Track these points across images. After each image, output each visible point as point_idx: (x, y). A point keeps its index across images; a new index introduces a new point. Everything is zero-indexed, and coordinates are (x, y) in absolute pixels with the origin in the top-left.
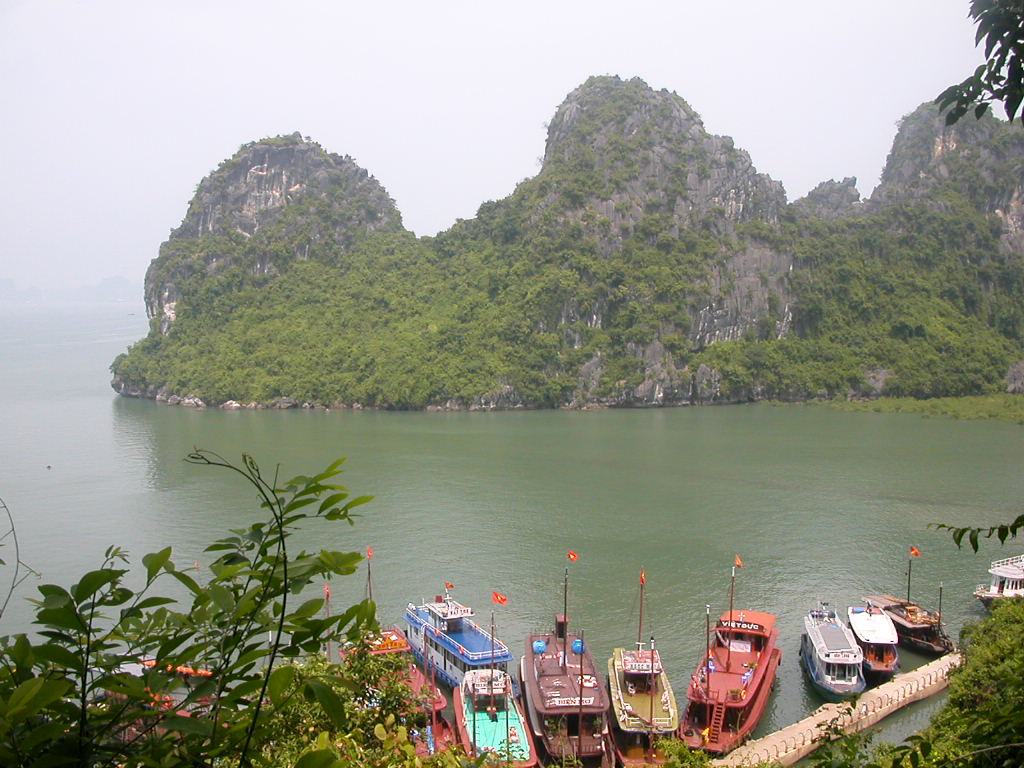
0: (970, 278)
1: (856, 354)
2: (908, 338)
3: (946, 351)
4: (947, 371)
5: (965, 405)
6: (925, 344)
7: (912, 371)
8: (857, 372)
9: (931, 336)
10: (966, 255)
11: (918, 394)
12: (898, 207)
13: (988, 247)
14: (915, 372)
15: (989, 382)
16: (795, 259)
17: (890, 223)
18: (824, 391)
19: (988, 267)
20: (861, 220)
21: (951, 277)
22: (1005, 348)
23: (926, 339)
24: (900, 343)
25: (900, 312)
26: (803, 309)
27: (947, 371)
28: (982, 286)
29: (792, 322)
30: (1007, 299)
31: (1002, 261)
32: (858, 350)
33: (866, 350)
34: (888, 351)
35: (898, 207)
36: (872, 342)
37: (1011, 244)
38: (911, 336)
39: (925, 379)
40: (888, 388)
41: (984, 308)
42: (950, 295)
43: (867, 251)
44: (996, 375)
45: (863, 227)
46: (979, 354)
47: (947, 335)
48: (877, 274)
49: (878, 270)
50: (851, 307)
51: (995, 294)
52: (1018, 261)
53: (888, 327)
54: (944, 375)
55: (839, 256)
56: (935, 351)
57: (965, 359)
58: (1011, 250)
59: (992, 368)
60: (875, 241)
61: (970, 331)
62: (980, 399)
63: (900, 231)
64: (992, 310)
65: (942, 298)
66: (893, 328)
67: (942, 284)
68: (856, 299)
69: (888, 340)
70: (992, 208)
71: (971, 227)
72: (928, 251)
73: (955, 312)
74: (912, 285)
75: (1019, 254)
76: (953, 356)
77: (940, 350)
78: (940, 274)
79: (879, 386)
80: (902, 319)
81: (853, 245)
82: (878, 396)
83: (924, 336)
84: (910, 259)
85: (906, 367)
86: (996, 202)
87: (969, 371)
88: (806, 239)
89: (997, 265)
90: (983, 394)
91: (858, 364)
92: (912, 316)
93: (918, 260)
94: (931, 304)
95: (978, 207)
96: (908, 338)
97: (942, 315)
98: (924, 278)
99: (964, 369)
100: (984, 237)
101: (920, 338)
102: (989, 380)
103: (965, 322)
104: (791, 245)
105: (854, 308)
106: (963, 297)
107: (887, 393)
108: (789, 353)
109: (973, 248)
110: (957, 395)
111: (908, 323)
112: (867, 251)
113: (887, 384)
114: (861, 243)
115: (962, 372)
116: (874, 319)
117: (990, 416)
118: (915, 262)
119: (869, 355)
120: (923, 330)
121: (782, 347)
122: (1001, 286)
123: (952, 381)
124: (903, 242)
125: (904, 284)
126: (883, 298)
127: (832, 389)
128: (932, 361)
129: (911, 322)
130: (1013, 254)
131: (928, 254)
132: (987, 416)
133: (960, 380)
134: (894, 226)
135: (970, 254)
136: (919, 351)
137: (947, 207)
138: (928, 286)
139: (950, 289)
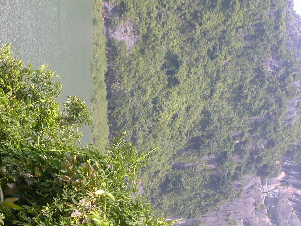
0: (221, 143)
1: (149, 14)
3: (154, 108)
4: (134, 108)
6: (161, 87)
7: (133, 71)
8: (131, 13)
9: (168, 94)
10: (244, 139)
12: (294, 68)
13: (251, 160)
14: (132, 74)
17: (277, 59)
19: (231, 161)
21: (223, 122)
22: (157, 172)
23: (164, 88)
25: (190, 65)
27: (134, 108)
28: (213, 156)
30: (199, 184)
31: (235, 177)
33: (153, 25)
34: (153, 47)
35: (294, 68)
36: (162, 32)
37: (252, 187)
38: (169, 73)
40: (116, 44)
41: (191, 158)
42: (206, 121)
43: (252, 32)
45: (277, 28)
48: (229, 42)
49: (233, 44)
50: (196, 12)
51: (204, 170)
53: (176, 51)
54: (130, 105)
56: (153, 97)
57: (145, 127)
58: (246, 188)
60: (262, 40)
63: (269, 69)
64: (188, 167)
65: (203, 112)
66: (176, 56)
67: (215, 112)
68: (205, 17)
69: (164, 49)
70: (286, 169)
71: (271, 144)
72: (249, 98)
73: (190, 122)
74: (218, 78)
75: (242, 195)
76: (149, 116)
77: (154, 102)
78: (226, 111)
79: (117, 36)
80: (185, 64)
81: (258, 16)
82: (107, 35)
83: (169, 86)
84: (242, 80)
85: (138, 64)
86: (292, 172)
87: (135, 131)
89: (232, 172)
92: (188, 76)
93: (240, 88)
94: (199, 99)
95: (289, 154)
96: (165, 71)
97: (188, 109)
98: (223, 93)
99: (137, 126)
100: (261, 157)
101: (166, 82)
103: (180, 133)
105: (195, 16)
106: (202, 136)
107: (110, 43)
109: (250, 147)
110: (110, 116)
111: (181, 70)
112: (252, 32)
114: (261, 25)
115: (134, 124)
116: (184, 37)
118: (239, 84)
119: (148, 28)
122: (211, 176)
123: (124, 114)
124: (259, 73)
125: (218, 71)
126: (204, 48)
128: (145, 92)
129: (182, 73)
131: (246, 97)
133: (125, 122)
134: (275, 63)
135: (245, 143)
136: (155, 79)
137: (290, 120)
138: (216, 97)
139: (212, 121)
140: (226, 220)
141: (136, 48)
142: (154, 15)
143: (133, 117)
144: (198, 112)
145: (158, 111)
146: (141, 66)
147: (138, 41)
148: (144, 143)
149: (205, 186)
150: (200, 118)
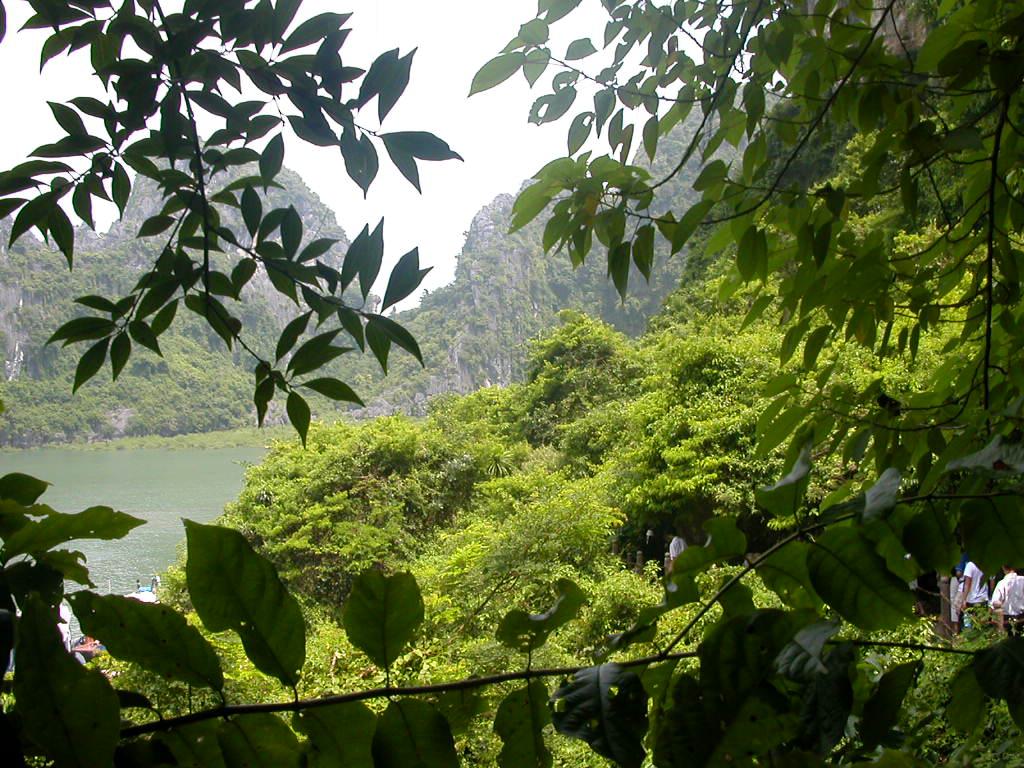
1: (96, 394)
2: (151, 375)
3: (191, 386)
4: (192, 407)
5: (212, 438)
8: (97, 412)
9: (175, 372)
11: (165, 432)
14: (158, 409)
15: (236, 416)
16: (25, 292)
17: (129, 259)
18: (62, 434)
20: (100, 254)
23: (170, 376)
24: (142, 381)
26: (36, 348)
27: (192, 407)
29: (23, 363)
30: (252, 338)
32: (97, 390)
33: (107, 390)
34: (131, 389)
38: (153, 372)
39: (170, 415)
44: (242, 408)
45: (100, 261)
46: (224, 389)
47: (191, 372)
52: (261, 299)
54: (190, 411)
55: (73, 290)
59: (238, 401)
60: (112, 276)
61: (215, 367)
62: (228, 434)
63: (139, 267)
65: (185, 336)
67: (184, 322)
73: (199, 349)
75: (261, 293)
76: (198, 392)
77: (185, 387)
79: (122, 426)
82: (121, 436)
83: (167, 372)
85: (149, 404)
88: (38, 271)
90: (230, 428)
91: (97, 404)
96: (151, 375)
97: (185, 352)
99: (210, 403)
102: (236, 414)
103: (210, 359)
104: (20, 278)
107: (129, 433)
108: (20, 396)
111: (150, 360)
113: (130, 423)
117: (238, 445)
120: (166, 367)
121: (13, 389)
127: (71, 432)
128: (176, 396)
130: (258, 294)
132: (234, 445)
133: (207, 415)
136: (162, 387)
140: (286, 308)
141: (131, 407)
142: (97, 390)
143: (202, 407)
144: (185, 340)
145: (194, 382)
146: (151, 401)
147: (124, 404)
148: (225, 396)
149: (254, 331)
150: (191, 339)
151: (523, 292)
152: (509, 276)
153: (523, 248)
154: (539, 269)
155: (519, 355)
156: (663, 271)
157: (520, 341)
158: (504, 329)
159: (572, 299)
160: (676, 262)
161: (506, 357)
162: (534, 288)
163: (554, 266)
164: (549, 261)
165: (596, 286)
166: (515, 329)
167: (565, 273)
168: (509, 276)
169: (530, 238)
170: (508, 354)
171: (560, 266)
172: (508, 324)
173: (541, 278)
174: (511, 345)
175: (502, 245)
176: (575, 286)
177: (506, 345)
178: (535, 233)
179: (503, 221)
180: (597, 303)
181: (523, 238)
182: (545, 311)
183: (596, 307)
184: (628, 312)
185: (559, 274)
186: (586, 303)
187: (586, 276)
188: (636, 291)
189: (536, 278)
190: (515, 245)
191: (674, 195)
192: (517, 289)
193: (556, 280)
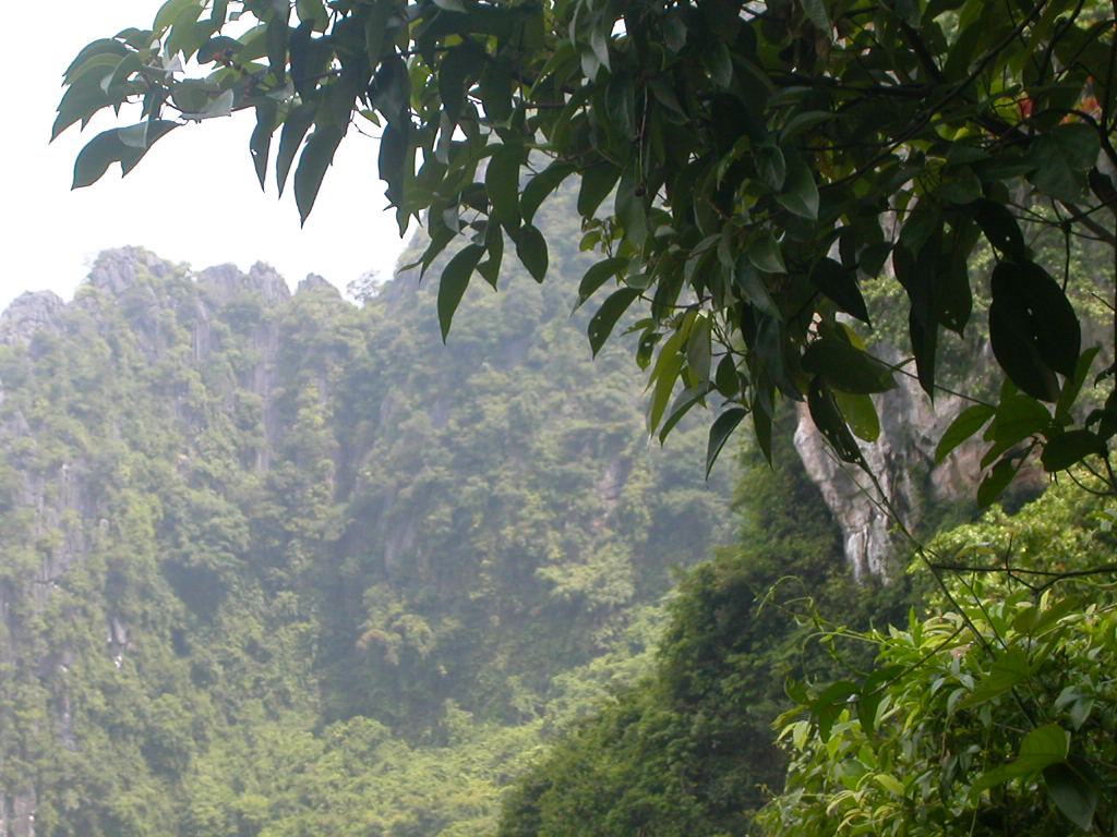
151: (86, 595)
152: (44, 549)
153: (88, 459)
154: (134, 521)
155: (61, 786)
156: (501, 539)
157: (69, 741)
158: (20, 705)
159: (230, 612)
160: (541, 516)
161: (23, 792)
162: (116, 579)
163: (182, 513)
164: (166, 499)
165: (304, 574)
166: (55, 704)
167: (213, 536)
168: (44, 549)
169: (112, 430)
170: (28, 783)
171: (199, 514)
172: (35, 692)
173: (139, 550)
174: (39, 755)
175: (25, 452)
176: (241, 572)
177: (24, 756)
178: (128, 414)
179: (33, 380)
180: (303, 627)
181: (91, 428)
182: (148, 651)
183: (304, 638)
184: (395, 659)
185: (193, 539)
186: (271, 624)
187: (277, 543)
188: (421, 596)
189: (124, 551)
190: (65, 451)
191: (546, 317)
192: (65, 584)
193: (186, 556)
